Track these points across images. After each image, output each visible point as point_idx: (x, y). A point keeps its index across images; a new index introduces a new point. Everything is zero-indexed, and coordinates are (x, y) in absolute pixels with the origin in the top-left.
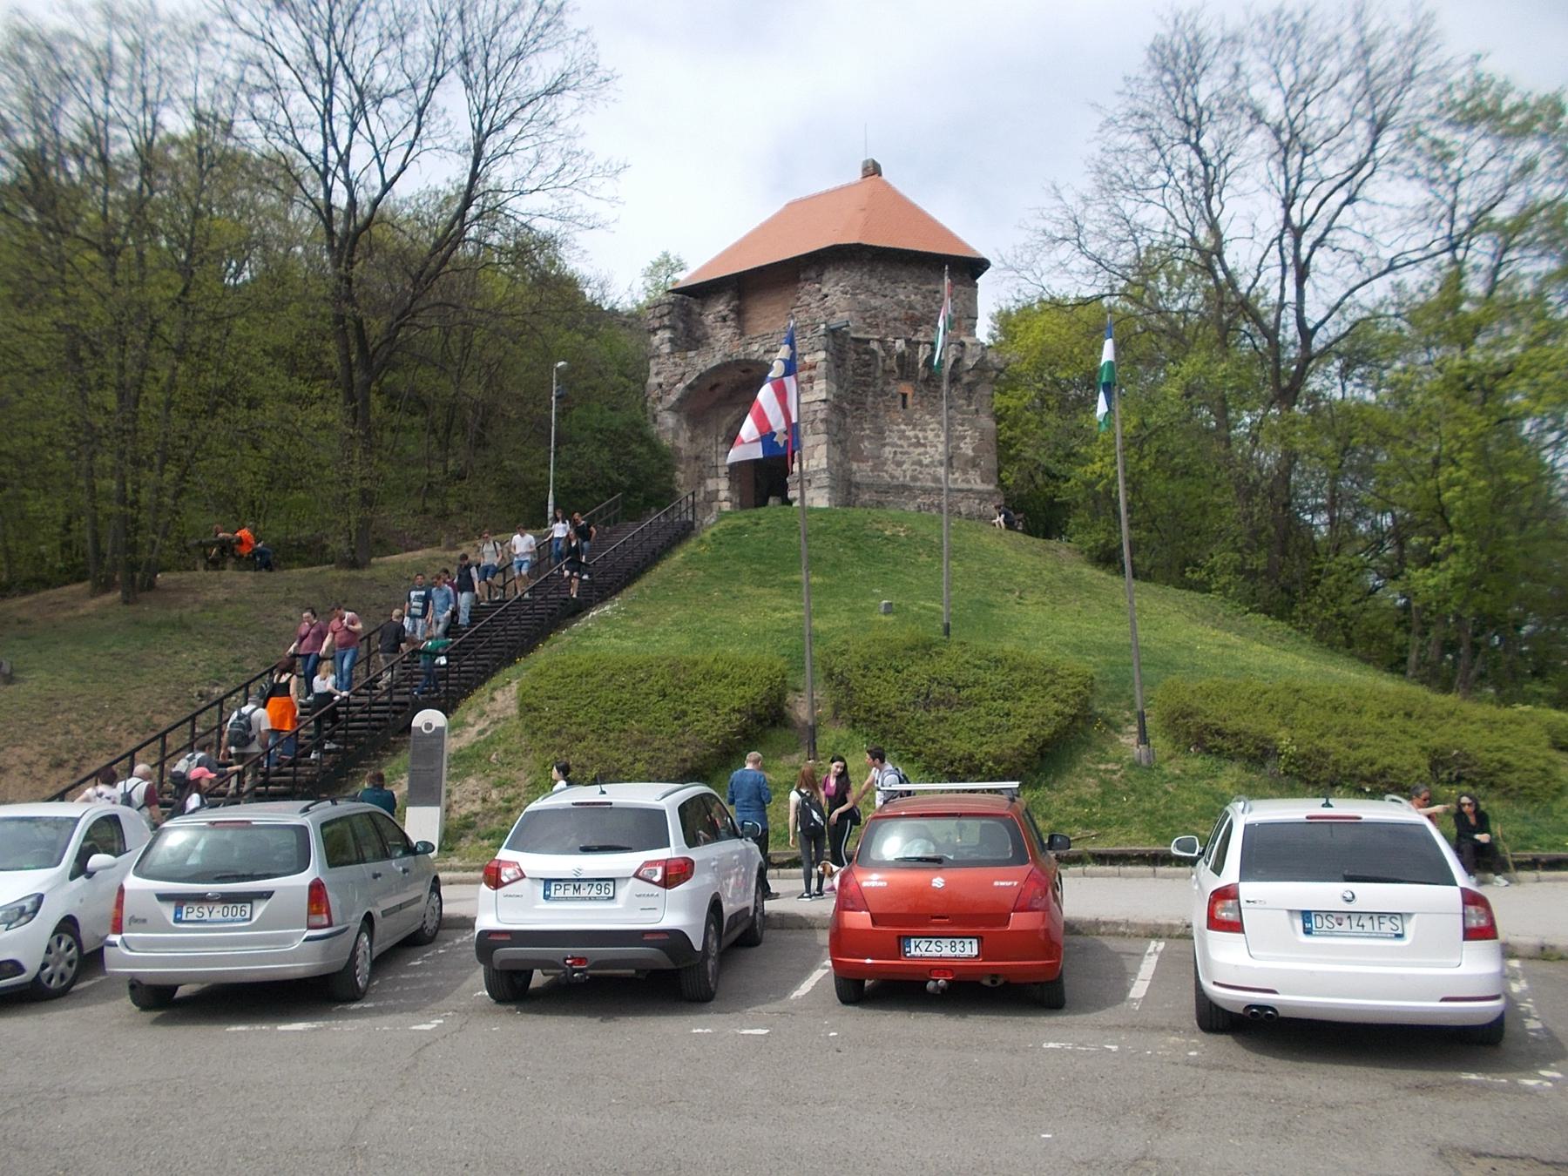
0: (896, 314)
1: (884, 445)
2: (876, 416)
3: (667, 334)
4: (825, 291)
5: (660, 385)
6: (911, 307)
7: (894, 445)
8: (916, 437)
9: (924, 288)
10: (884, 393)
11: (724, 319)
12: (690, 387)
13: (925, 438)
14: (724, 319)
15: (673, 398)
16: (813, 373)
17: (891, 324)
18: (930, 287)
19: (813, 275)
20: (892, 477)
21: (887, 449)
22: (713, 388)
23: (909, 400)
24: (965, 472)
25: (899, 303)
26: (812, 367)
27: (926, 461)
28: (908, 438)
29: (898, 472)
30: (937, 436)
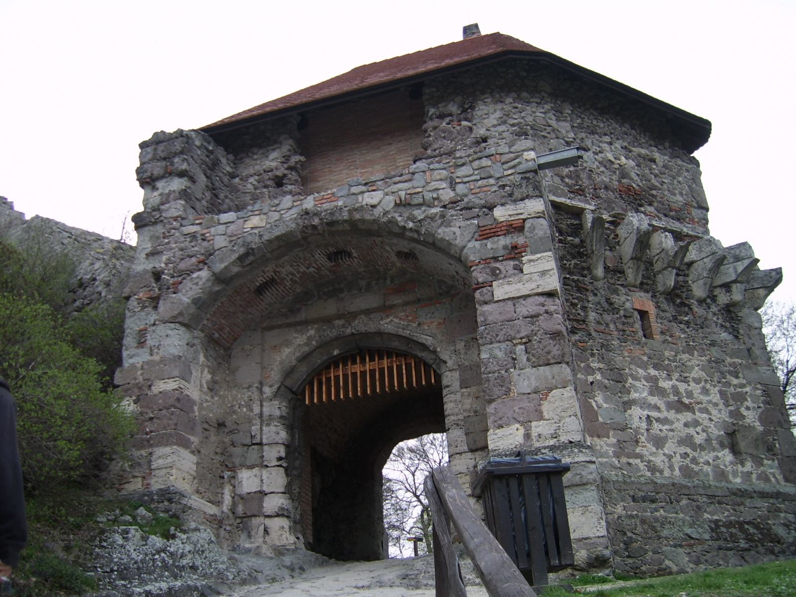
1: (628, 405)
2: (606, 347)
3: (177, 184)
4: (481, 132)
5: (157, 275)
6: (624, 174)
8: (676, 392)
9: (636, 150)
10: (612, 308)
11: (279, 182)
13: (690, 394)
14: (279, 182)
15: (187, 294)
16: (520, 240)
17: (602, 193)
18: (643, 151)
19: (453, 108)
20: (653, 468)
21: (636, 412)
23: (656, 326)
24: (759, 462)
25: (607, 164)
26: (517, 227)
27: (699, 439)
28: (662, 392)
29: (659, 460)
30: (705, 392)
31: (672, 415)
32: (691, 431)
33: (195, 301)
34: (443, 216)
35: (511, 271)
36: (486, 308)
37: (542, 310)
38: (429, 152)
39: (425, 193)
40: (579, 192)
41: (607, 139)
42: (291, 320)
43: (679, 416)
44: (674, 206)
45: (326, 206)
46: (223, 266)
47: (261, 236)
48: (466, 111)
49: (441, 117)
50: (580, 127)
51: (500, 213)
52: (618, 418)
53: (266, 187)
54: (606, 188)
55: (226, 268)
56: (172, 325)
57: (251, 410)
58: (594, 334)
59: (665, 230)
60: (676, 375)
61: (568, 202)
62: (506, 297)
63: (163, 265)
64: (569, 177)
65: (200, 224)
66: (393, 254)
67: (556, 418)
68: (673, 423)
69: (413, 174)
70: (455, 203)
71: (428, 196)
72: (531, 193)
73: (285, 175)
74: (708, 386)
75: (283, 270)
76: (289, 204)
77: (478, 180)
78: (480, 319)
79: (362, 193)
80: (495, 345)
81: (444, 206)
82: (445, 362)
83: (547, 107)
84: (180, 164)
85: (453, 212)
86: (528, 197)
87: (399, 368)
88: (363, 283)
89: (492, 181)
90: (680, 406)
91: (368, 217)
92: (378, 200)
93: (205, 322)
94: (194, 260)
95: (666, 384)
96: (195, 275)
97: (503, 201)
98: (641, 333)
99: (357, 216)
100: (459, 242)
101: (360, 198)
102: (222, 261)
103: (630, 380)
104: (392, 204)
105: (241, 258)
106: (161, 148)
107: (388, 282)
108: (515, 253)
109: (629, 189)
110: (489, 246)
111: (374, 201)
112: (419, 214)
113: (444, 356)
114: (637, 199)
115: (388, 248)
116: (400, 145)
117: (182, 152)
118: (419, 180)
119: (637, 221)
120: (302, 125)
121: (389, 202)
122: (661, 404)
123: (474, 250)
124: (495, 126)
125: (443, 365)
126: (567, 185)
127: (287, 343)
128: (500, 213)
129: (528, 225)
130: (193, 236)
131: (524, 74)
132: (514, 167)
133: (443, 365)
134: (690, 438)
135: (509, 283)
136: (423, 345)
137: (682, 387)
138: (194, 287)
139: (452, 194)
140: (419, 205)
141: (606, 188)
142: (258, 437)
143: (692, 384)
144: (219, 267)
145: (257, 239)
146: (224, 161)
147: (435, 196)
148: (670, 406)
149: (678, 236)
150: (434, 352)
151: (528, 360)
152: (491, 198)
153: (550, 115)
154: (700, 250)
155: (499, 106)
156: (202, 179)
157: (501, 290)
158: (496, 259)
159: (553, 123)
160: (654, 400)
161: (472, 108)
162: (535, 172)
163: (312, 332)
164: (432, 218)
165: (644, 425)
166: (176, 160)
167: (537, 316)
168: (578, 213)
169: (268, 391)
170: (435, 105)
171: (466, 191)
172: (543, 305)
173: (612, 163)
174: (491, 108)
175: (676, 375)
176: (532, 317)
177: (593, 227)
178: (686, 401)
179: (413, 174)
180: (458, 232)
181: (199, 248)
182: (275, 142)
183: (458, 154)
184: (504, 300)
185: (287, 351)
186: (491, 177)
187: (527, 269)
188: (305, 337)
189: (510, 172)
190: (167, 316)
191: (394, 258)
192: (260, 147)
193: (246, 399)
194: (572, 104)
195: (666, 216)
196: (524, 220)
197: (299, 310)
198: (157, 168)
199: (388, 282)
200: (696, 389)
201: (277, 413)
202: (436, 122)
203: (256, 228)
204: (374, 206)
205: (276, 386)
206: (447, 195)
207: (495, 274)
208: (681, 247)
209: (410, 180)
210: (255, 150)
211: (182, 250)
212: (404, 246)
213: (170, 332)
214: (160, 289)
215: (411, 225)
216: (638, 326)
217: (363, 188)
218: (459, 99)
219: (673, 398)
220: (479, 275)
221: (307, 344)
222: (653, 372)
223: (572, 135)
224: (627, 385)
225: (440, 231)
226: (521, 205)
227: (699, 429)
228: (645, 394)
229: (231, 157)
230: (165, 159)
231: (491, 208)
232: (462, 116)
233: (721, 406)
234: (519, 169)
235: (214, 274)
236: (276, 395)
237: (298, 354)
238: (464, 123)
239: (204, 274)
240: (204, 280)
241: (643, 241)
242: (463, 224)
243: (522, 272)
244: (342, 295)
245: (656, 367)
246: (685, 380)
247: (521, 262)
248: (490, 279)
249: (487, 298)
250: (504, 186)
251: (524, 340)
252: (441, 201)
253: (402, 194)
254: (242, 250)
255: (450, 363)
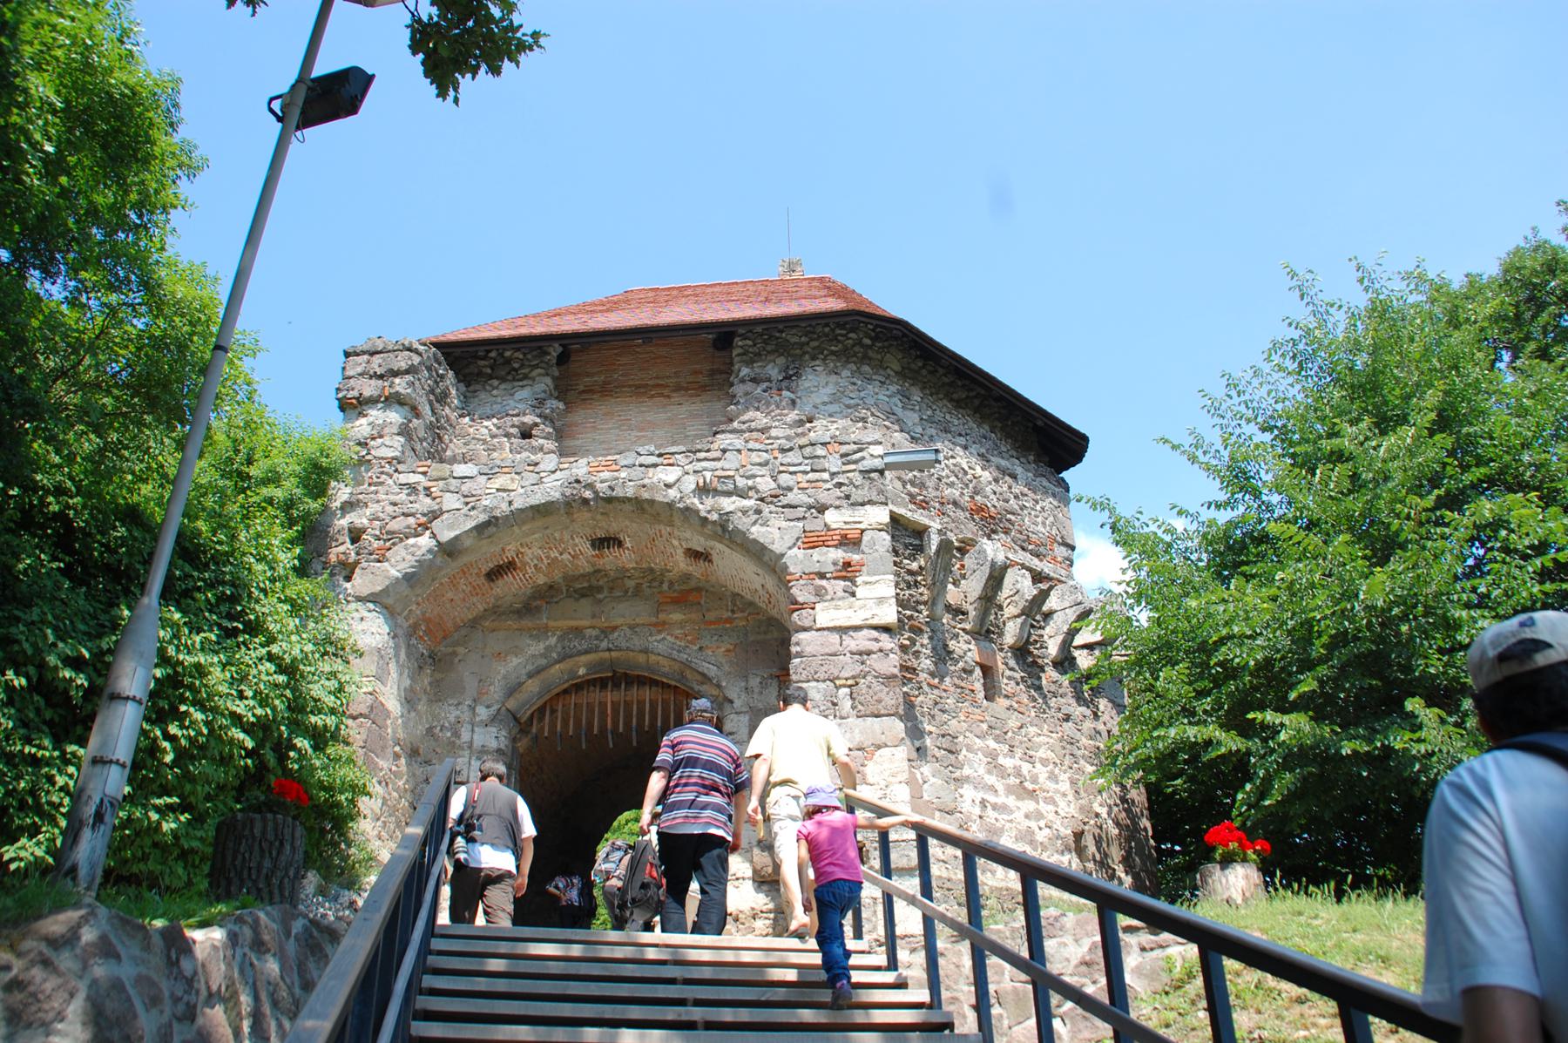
0: (954, 493)
3: (394, 417)
7: (979, 785)
8: (1018, 772)
12: (448, 550)
13: (1035, 780)
15: (399, 563)
16: (856, 557)
18: (1003, 463)
19: (773, 371)
21: (968, 792)
22: (494, 574)
26: (849, 541)
27: (1041, 836)
30: (1053, 777)
31: (1011, 801)
32: (1033, 825)
33: (408, 578)
34: (758, 512)
35: (840, 594)
36: (802, 636)
37: (874, 646)
38: (735, 424)
39: (737, 478)
40: (924, 505)
41: (962, 440)
42: (527, 622)
43: (1020, 804)
44: (1034, 537)
45: (606, 475)
46: (452, 534)
47: (510, 503)
48: (790, 377)
49: (756, 381)
50: (931, 420)
51: (833, 518)
52: (947, 799)
53: (507, 435)
54: (955, 503)
55: (456, 537)
56: (371, 606)
57: (459, 737)
58: (926, 688)
59: (1023, 566)
60: (1019, 752)
61: (909, 514)
62: (831, 625)
63: (365, 521)
64: (913, 484)
65: (424, 473)
66: (680, 551)
67: (883, 784)
68: (1012, 812)
69: (724, 451)
70: (776, 496)
71: (741, 482)
72: (874, 498)
73: (536, 425)
74: (1057, 771)
75: (529, 552)
76: (552, 467)
77: (806, 473)
78: (794, 649)
79: (655, 465)
80: (813, 684)
81: (762, 500)
82: (731, 702)
83: (894, 388)
84: (400, 385)
85: (772, 508)
86: (870, 502)
87: (665, 703)
88: (631, 584)
89: (826, 476)
90: (1024, 791)
91: (659, 498)
92: (673, 479)
93: (414, 607)
94: (411, 520)
95: (1007, 762)
96: (411, 541)
97: (838, 503)
98: (982, 694)
99: (646, 495)
100: (777, 548)
101: (651, 470)
102: (451, 527)
103: (964, 752)
104: (693, 486)
105: (480, 528)
106: (377, 359)
107: (665, 586)
108: (847, 571)
109: (981, 509)
110: (815, 558)
111: (671, 479)
112: (728, 504)
113: (732, 693)
114: (992, 523)
115: (676, 543)
116: (693, 407)
117: (407, 372)
118: (731, 462)
119: (994, 549)
120: (563, 359)
121: (690, 483)
122: (1000, 787)
123: (797, 560)
124: (825, 403)
125: (727, 706)
126: (910, 494)
127: (516, 651)
128: (833, 518)
129: (866, 538)
130: (413, 489)
131: (868, 342)
132: (856, 462)
133: (727, 706)
134: (1029, 831)
135: (837, 608)
136: (703, 675)
137: (1026, 768)
138: (409, 557)
139: (773, 485)
140: (728, 494)
141: (955, 503)
142: (465, 773)
143: (1038, 765)
144: (446, 535)
145: (504, 506)
146: (454, 392)
147: (750, 483)
148: (1010, 790)
149: (1038, 577)
150: (719, 686)
151: (853, 708)
152: (824, 497)
153: (896, 400)
154: (1062, 597)
155: (834, 378)
156: (426, 410)
157: (826, 615)
158: (822, 576)
159: (899, 411)
160: (991, 780)
161: (798, 375)
162: (881, 472)
163: (553, 640)
164: (745, 512)
165: (977, 811)
166: (397, 381)
167: (869, 653)
168: (920, 532)
169: (483, 713)
170: (749, 363)
171: (791, 483)
172: (876, 640)
173: (966, 473)
174: (823, 378)
175: (1019, 752)
176: (860, 654)
177: (938, 552)
178: (1029, 786)
179: (724, 451)
180: (775, 533)
181: (425, 503)
182: (526, 377)
183: (774, 433)
184: (828, 629)
185: (515, 661)
186: (824, 470)
187: (860, 592)
188: (542, 646)
189: (853, 467)
190: (365, 592)
191: (680, 556)
192: (503, 380)
193: (452, 719)
194: (922, 389)
195: (1023, 549)
196: (863, 531)
197: (538, 609)
198: (369, 388)
199: (665, 586)
200: (1042, 772)
201: (494, 744)
202: (749, 386)
203: (505, 490)
204: (668, 486)
205: (496, 707)
206: (766, 484)
207: (820, 593)
208: (1042, 591)
209: (719, 459)
210: (496, 383)
211: (395, 504)
212: (698, 543)
213: (366, 614)
214: (358, 554)
215: (714, 517)
216: (978, 686)
217: (659, 460)
218: (781, 361)
219: (1013, 781)
220: (801, 593)
221: (544, 655)
222: (992, 744)
223: (919, 429)
224: (961, 757)
225: (753, 529)
226: (861, 511)
227: (1042, 823)
228: (982, 771)
229: (462, 387)
230: (381, 377)
231: (822, 509)
232: (784, 384)
233: (1071, 797)
234: (860, 466)
235: (439, 544)
236: (493, 720)
237: (530, 668)
238: (785, 393)
239: (425, 541)
240: (424, 550)
241: (996, 578)
242: (784, 524)
243: (853, 594)
244: (600, 596)
245: (997, 739)
246: (1030, 760)
247: (854, 583)
248: (813, 599)
249: (807, 623)
250: (840, 485)
251: (850, 682)
252: (757, 492)
253: (708, 475)
254: (483, 518)
255: (737, 703)
